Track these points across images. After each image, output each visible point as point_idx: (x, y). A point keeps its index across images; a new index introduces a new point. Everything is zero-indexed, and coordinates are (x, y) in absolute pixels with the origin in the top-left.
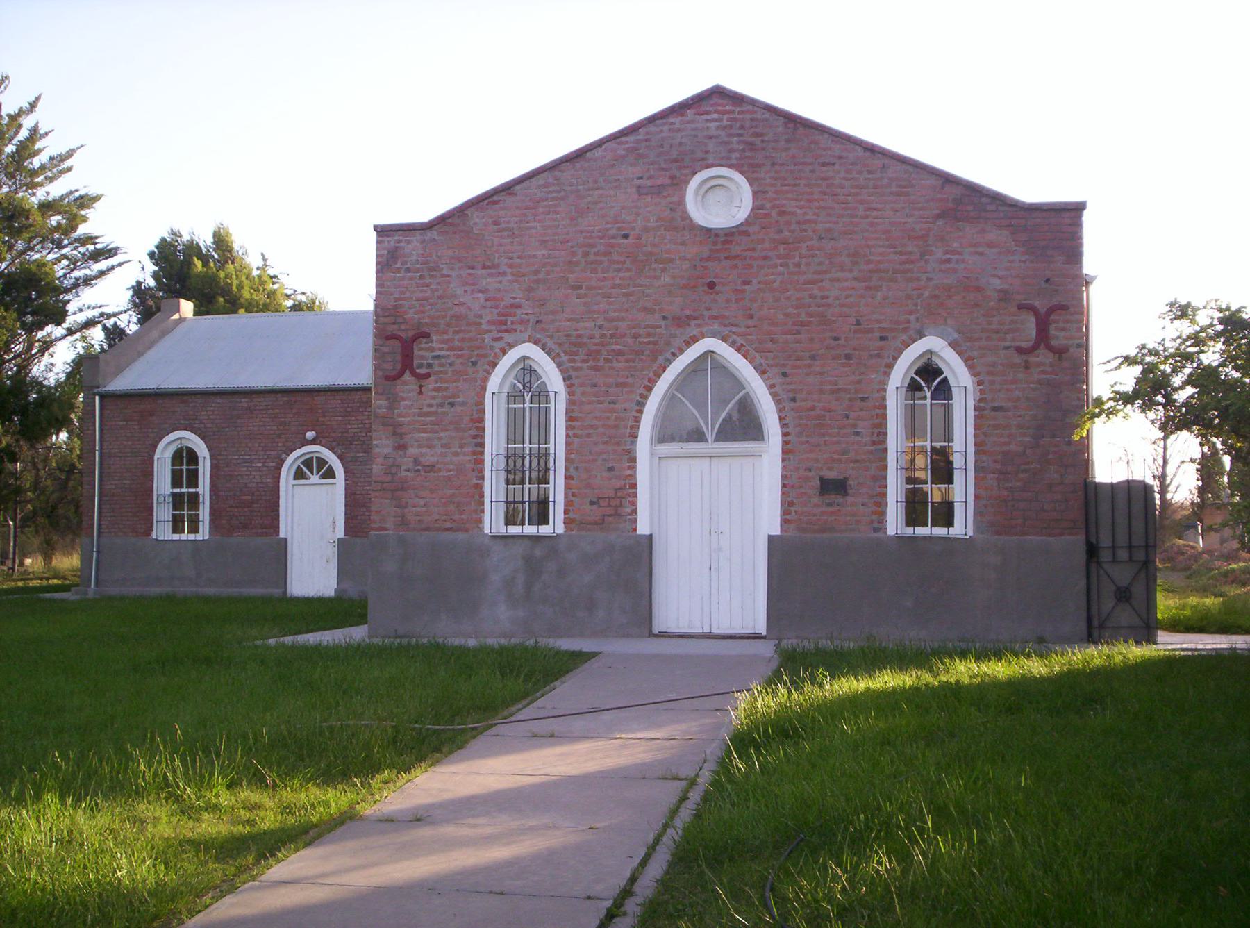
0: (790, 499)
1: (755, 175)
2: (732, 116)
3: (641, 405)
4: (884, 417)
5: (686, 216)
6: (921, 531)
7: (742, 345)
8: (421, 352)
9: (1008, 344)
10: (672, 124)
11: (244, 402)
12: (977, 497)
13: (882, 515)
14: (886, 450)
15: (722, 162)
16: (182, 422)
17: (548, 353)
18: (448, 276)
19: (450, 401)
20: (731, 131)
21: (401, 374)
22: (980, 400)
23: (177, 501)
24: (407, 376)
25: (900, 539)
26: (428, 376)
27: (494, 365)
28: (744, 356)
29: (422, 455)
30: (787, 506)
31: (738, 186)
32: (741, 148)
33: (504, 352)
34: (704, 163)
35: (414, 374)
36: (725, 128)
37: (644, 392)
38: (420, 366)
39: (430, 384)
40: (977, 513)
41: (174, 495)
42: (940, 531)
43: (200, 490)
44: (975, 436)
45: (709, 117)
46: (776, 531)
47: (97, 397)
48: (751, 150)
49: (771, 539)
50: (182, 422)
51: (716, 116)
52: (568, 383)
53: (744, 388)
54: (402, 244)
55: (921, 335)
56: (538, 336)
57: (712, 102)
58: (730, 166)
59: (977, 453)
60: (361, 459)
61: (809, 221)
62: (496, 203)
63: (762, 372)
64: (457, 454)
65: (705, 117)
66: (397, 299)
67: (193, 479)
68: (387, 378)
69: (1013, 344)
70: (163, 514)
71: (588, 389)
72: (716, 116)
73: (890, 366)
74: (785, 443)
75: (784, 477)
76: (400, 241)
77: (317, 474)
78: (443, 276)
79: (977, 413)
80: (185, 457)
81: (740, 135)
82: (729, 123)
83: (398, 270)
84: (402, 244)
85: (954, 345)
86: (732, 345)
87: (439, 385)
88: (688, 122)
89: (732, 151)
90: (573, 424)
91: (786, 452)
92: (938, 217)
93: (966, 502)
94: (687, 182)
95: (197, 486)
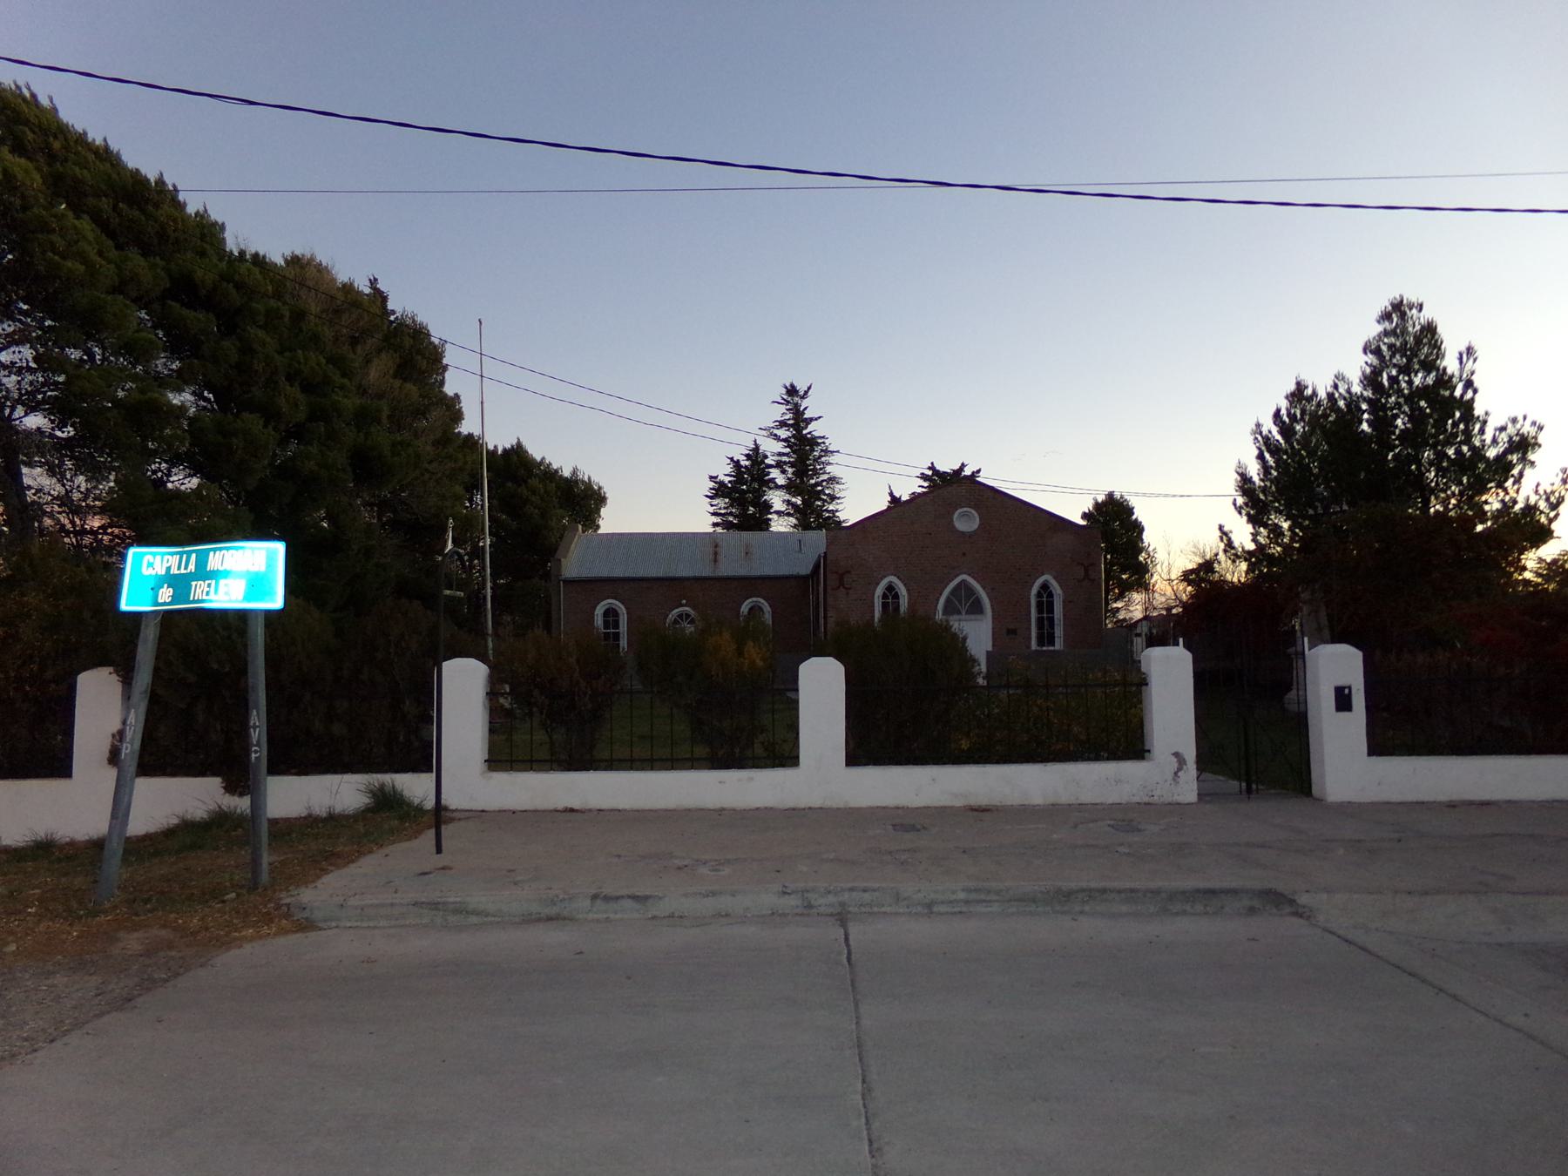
3: (938, 600)
4: (1030, 605)
5: (954, 527)
6: (1044, 648)
12: (1064, 635)
13: (1030, 642)
21: (839, 587)
24: (841, 588)
25: (1036, 651)
26: (850, 589)
27: (878, 584)
30: (994, 639)
31: (973, 515)
33: (882, 579)
35: (844, 587)
39: (851, 592)
40: (1064, 641)
43: (621, 630)
46: (990, 649)
47: (561, 583)
49: (988, 652)
55: (1043, 574)
63: (984, 588)
67: (616, 625)
68: (833, 589)
73: (1032, 586)
74: (993, 616)
75: (993, 628)
77: (682, 620)
80: (611, 614)
85: (1055, 578)
86: (973, 577)
91: (994, 618)
94: (953, 513)
95: (618, 628)
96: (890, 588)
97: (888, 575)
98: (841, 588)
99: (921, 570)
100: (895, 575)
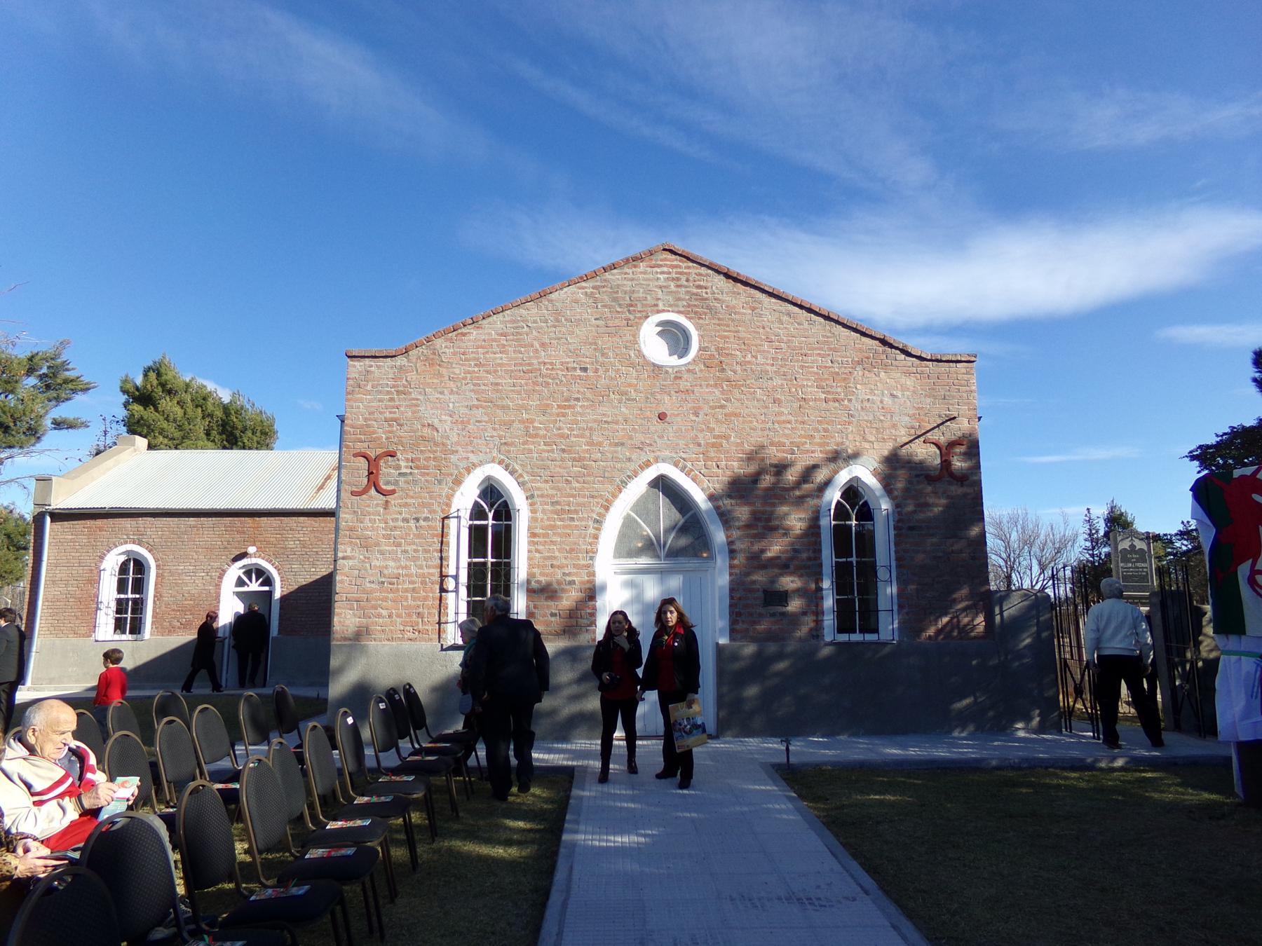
0: (737, 610)
1: (701, 321)
2: (679, 270)
3: (599, 522)
5: (640, 354)
7: (692, 470)
8: (387, 472)
9: (919, 473)
10: (626, 273)
11: (192, 521)
14: (821, 565)
15: (670, 309)
16: (131, 537)
17: (512, 473)
18: (417, 399)
19: (414, 516)
20: (679, 283)
21: (365, 491)
22: (899, 521)
23: (121, 606)
26: (393, 492)
28: (692, 479)
29: (386, 567)
32: (687, 297)
34: (656, 308)
36: (673, 279)
37: (602, 511)
38: (388, 483)
41: (119, 602)
42: (870, 637)
44: (896, 552)
45: (659, 270)
48: (696, 300)
50: (131, 537)
51: (665, 269)
52: (530, 501)
53: (692, 509)
54: (373, 369)
56: (502, 457)
57: (662, 257)
58: (679, 312)
59: (898, 567)
60: (296, 570)
61: (749, 362)
62: (464, 334)
64: (421, 567)
65: (655, 269)
66: (366, 420)
68: (353, 493)
69: (922, 472)
70: (106, 620)
71: (549, 507)
72: (665, 269)
76: (371, 366)
78: (414, 399)
79: (896, 532)
81: (686, 287)
82: (677, 276)
83: (369, 393)
84: (373, 369)
87: (404, 500)
88: (641, 273)
89: (679, 299)
90: (535, 540)
92: (860, 363)
93: (892, 610)
96: (491, 492)
97: (481, 463)
98: (373, 492)
99: (563, 451)
100: (500, 463)
